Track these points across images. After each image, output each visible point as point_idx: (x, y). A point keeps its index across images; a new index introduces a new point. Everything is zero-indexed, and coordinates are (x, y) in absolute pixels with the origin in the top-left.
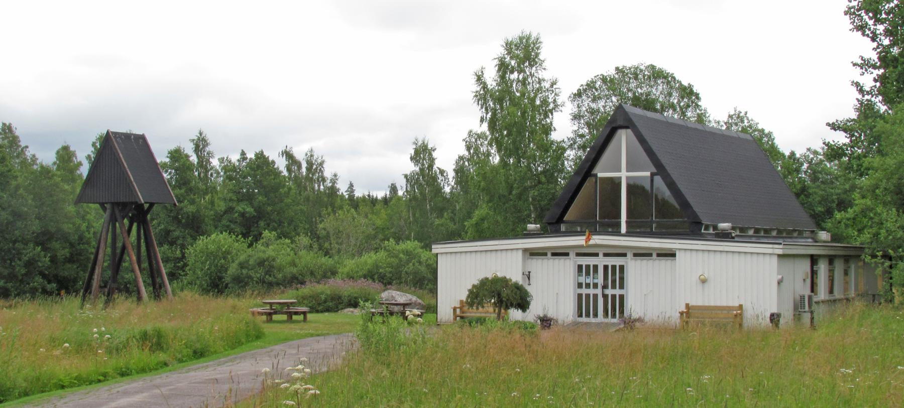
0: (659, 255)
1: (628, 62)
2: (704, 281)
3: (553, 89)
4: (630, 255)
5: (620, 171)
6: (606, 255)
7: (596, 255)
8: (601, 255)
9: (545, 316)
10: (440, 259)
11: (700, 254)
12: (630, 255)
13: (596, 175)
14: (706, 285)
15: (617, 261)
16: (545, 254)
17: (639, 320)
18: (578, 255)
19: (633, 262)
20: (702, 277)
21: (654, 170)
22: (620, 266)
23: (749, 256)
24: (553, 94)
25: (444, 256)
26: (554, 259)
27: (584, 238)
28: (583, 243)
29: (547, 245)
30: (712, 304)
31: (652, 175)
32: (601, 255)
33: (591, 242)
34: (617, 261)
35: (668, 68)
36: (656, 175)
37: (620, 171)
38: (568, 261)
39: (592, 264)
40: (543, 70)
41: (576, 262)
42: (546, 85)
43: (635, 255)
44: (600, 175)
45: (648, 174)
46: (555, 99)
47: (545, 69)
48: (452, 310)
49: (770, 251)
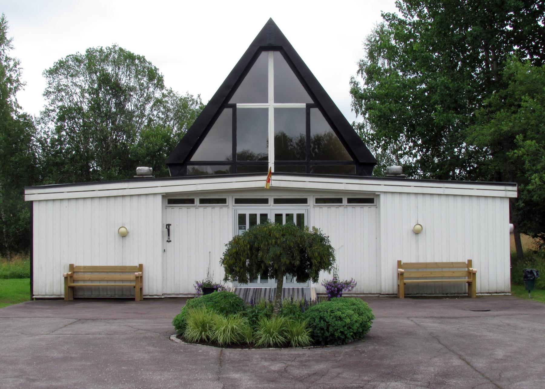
0: (350, 201)
1: (96, 45)
2: (417, 233)
3: (17, 69)
4: (311, 201)
5: (267, 102)
6: (277, 201)
7: (265, 201)
8: (271, 201)
9: (209, 284)
10: (35, 207)
11: (413, 197)
12: (311, 201)
13: (234, 106)
14: (420, 236)
15: (294, 210)
16: (192, 201)
17: (347, 284)
18: (238, 201)
19: (317, 209)
20: (123, 230)
21: (311, 101)
22: (250, 215)
23: (475, 200)
24: (16, 74)
25: (43, 204)
26: (205, 207)
27: (265, 178)
28: (263, 184)
29: (200, 188)
30: (429, 260)
31: (309, 107)
32: (271, 201)
33: (274, 184)
34: (294, 210)
35: (136, 51)
36: (311, 107)
37: (267, 102)
38: (225, 210)
39: (284, 213)
40: (10, 49)
41: (235, 211)
42: (12, 63)
43: (318, 201)
44: (239, 106)
45: (303, 105)
46: (18, 78)
47: (11, 48)
48: (63, 279)
49: (502, 194)
